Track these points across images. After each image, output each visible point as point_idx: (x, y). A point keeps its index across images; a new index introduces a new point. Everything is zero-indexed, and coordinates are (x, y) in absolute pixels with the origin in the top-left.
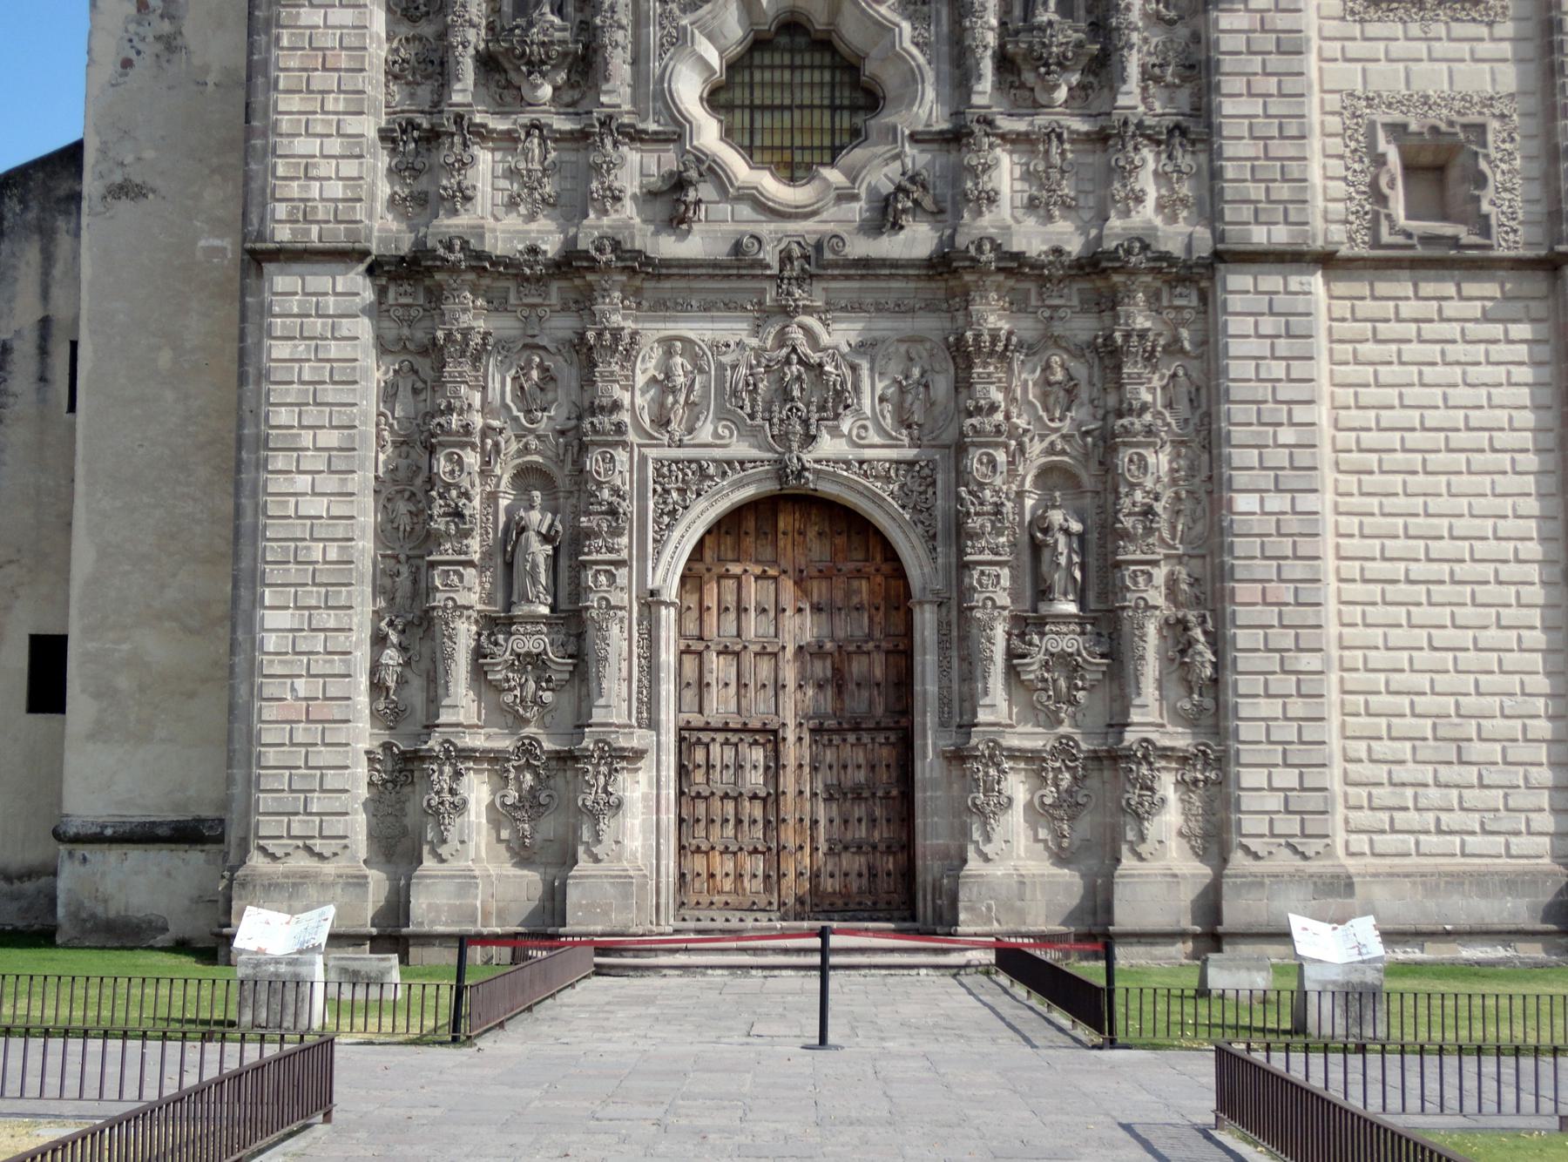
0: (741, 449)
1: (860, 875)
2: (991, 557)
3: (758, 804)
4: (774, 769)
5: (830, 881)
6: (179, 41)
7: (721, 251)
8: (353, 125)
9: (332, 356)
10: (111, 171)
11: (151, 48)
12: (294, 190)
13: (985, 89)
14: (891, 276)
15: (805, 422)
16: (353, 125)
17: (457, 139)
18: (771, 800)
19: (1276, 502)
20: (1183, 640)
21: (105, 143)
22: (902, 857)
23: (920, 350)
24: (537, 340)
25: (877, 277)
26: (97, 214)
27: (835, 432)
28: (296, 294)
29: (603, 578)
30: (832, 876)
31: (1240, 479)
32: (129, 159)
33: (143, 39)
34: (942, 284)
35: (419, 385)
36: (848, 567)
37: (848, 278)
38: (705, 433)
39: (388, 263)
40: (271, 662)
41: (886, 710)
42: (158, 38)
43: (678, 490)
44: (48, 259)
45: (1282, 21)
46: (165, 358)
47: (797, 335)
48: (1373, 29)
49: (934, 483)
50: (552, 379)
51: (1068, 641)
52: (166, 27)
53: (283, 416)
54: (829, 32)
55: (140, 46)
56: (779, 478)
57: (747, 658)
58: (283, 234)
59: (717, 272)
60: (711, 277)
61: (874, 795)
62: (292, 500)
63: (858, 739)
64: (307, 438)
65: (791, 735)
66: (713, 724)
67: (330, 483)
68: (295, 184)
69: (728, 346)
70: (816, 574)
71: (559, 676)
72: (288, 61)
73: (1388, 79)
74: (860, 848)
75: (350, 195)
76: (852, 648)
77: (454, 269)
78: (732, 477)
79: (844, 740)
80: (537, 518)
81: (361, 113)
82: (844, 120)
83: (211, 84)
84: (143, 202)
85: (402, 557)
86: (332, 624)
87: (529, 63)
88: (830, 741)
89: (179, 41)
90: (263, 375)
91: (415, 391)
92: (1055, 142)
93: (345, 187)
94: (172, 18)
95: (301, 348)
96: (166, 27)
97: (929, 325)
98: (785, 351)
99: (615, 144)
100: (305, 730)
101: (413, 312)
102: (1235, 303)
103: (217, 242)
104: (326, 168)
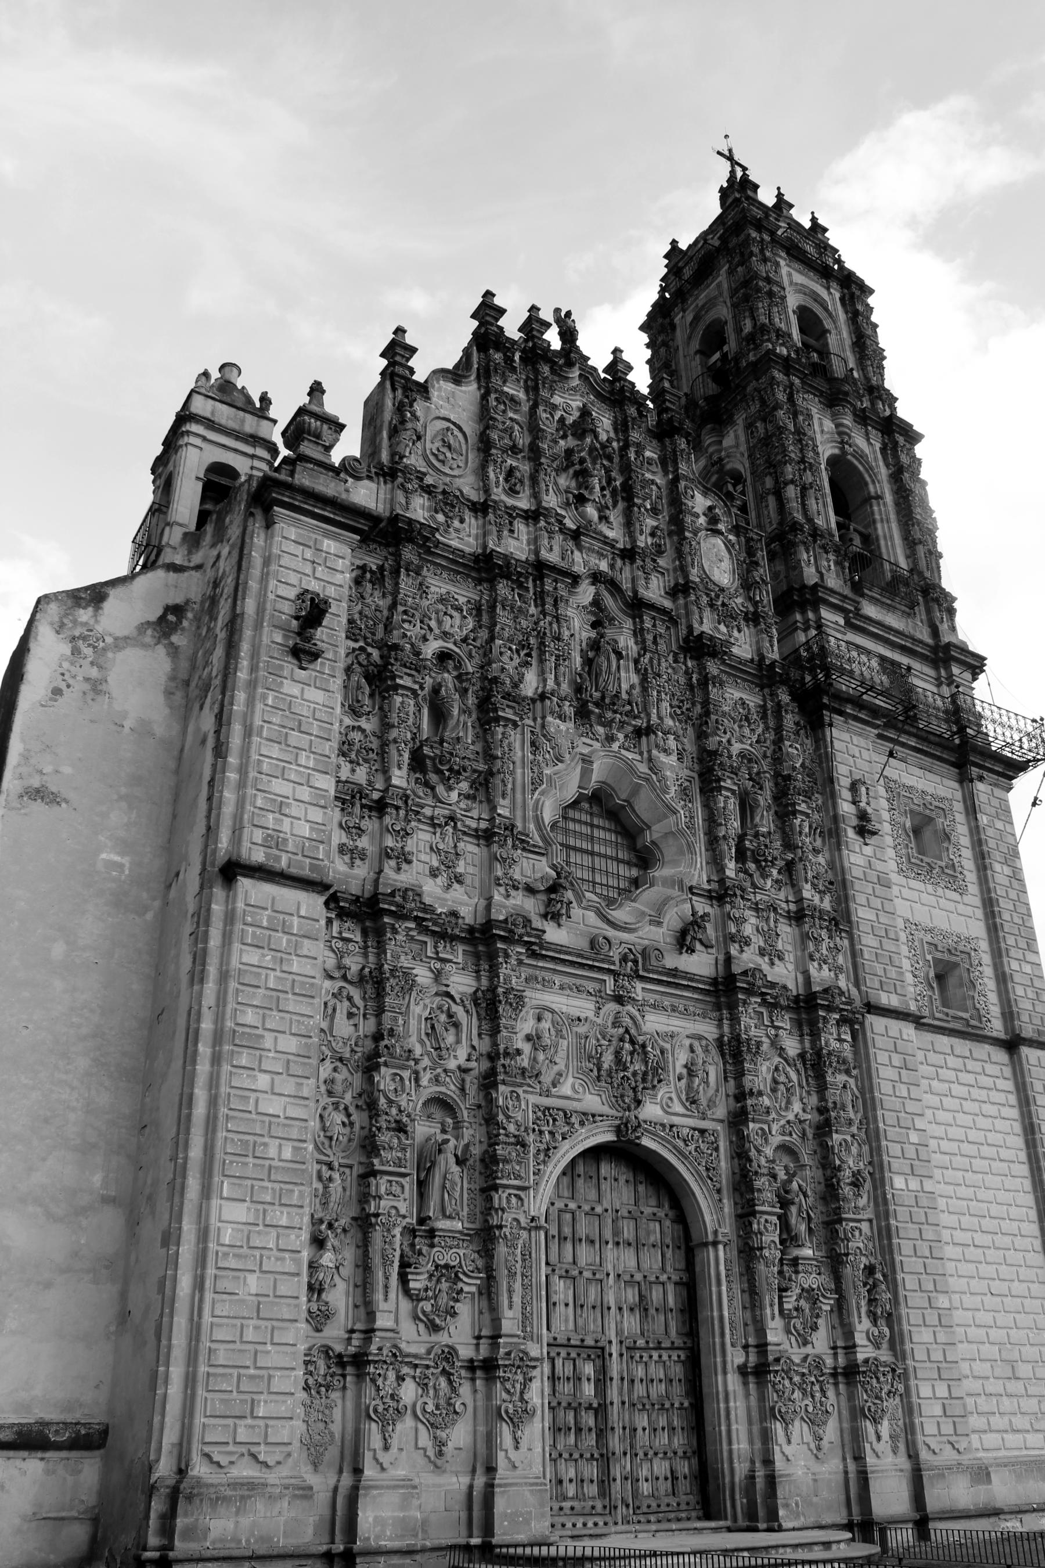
1: (666, 1479)
2: (769, 1209)
3: (591, 1413)
4: (602, 1380)
5: (645, 1484)
6: (104, 687)
9: (294, 969)
10: (30, 775)
11: (79, 686)
12: (270, 820)
13: (731, 868)
14: (687, 987)
15: (634, 1089)
17: (402, 812)
18: (601, 1410)
19: (914, 1184)
20: (871, 1282)
21: (29, 750)
22: (695, 1461)
23: (696, 1044)
24: (449, 989)
25: (677, 986)
26: (13, 809)
28: (266, 909)
29: (514, 1200)
30: (647, 1480)
31: (896, 1165)
32: (48, 769)
33: (74, 677)
34: (713, 1000)
35: (354, 1010)
36: (648, 1211)
37: (660, 982)
38: (566, 1089)
39: (345, 900)
40: (226, 1255)
41: (678, 1333)
42: (87, 680)
43: (550, 1132)
46: (58, 950)
48: (913, 883)
49: (717, 1149)
50: (457, 1025)
51: (811, 1280)
52: (94, 672)
54: (623, 807)
55: (71, 681)
56: (618, 1131)
57: (581, 1283)
58: (258, 856)
59: (579, 960)
60: (572, 963)
61: (672, 1405)
62: (253, 1095)
63: (660, 1356)
65: (614, 1349)
66: (559, 1341)
67: (288, 1086)
68: (271, 816)
69: (579, 1019)
70: (626, 1214)
71: (466, 1289)
73: (921, 916)
74: (665, 1453)
75: (315, 836)
76: (653, 1279)
78: (588, 1127)
79: (651, 1357)
81: (326, 773)
82: (624, 871)
83: (127, 730)
84: (56, 808)
85: (336, 1164)
86: (284, 1222)
87: (451, 770)
88: (641, 1357)
89: (104, 687)
91: (350, 1015)
92: (772, 914)
93: (311, 829)
94: (100, 667)
95: (268, 958)
96: (94, 672)
97: (708, 1029)
98: (621, 1030)
99: (514, 846)
100: (256, 1328)
101: (351, 947)
102: (880, 1042)
103: (117, 858)
104: (295, 810)
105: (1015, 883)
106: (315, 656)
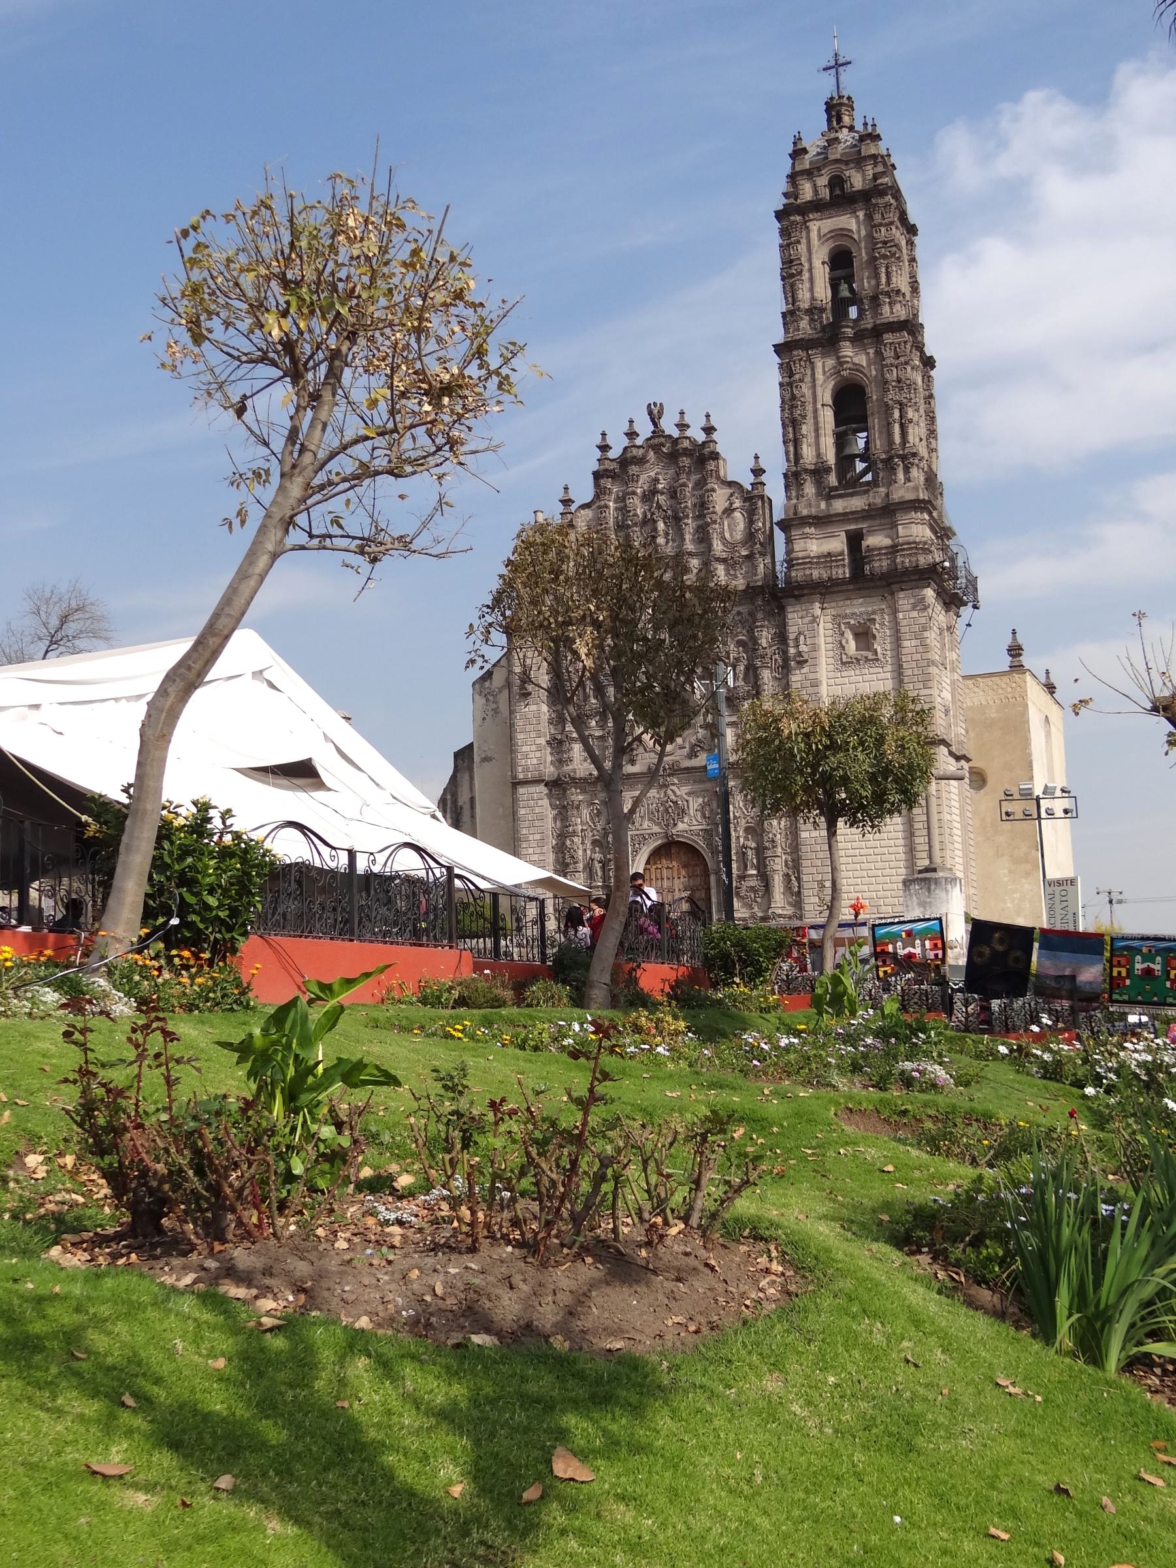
0: (656, 829)
7: (645, 770)
8: (539, 741)
11: (490, 713)
16: (539, 741)
27: (683, 822)
38: (645, 826)
44: (472, 778)
45: (811, 676)
46: (501, 811)
47: (669, 792)
48: (844, 674)
51: (753, 883)
52: (494, 706)
53: (524, 831)
58: (521, 776)
64: (531, 837)
67: (538, 850)
72: (519, 723)
77: (567, 783)
80: (598, 856)
90: (519, 819)
105: (920, 649)
106: (530, 694)
